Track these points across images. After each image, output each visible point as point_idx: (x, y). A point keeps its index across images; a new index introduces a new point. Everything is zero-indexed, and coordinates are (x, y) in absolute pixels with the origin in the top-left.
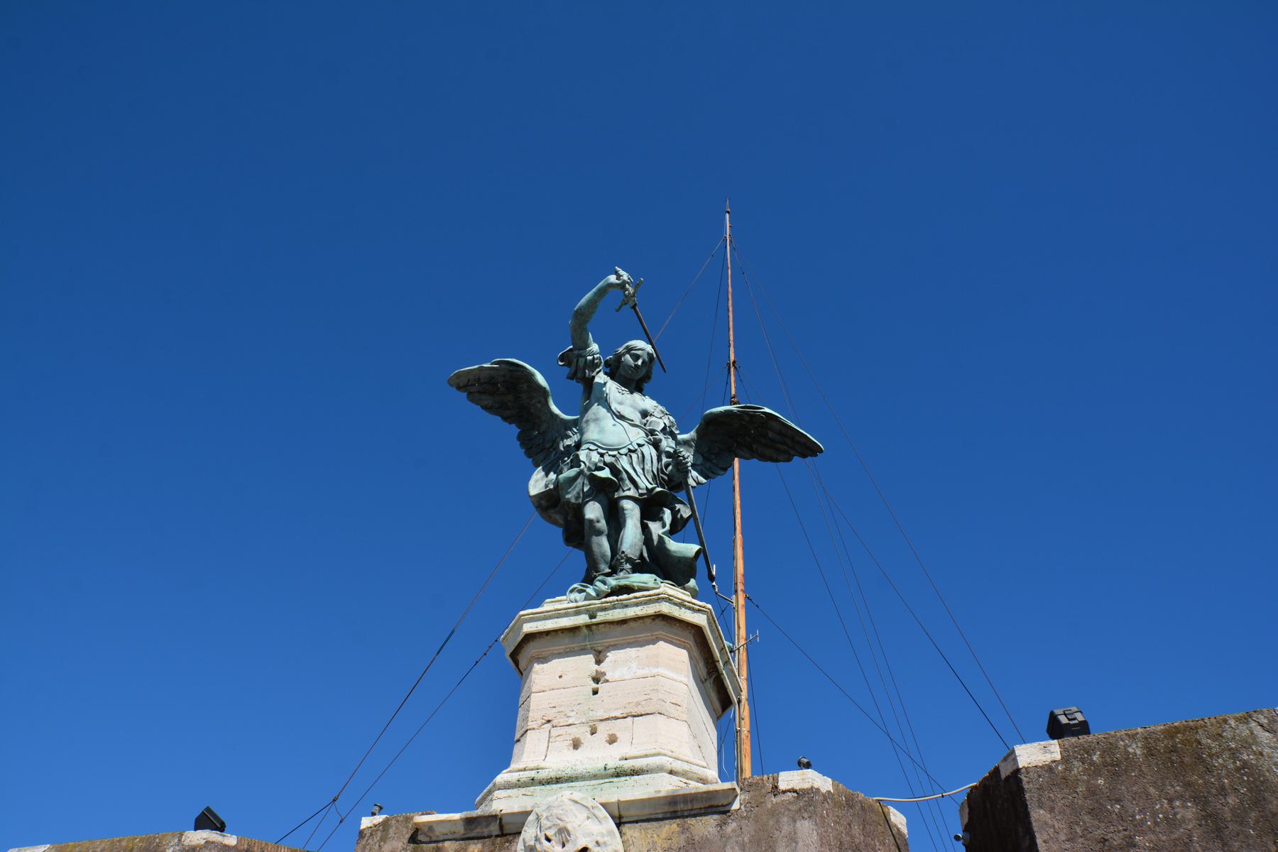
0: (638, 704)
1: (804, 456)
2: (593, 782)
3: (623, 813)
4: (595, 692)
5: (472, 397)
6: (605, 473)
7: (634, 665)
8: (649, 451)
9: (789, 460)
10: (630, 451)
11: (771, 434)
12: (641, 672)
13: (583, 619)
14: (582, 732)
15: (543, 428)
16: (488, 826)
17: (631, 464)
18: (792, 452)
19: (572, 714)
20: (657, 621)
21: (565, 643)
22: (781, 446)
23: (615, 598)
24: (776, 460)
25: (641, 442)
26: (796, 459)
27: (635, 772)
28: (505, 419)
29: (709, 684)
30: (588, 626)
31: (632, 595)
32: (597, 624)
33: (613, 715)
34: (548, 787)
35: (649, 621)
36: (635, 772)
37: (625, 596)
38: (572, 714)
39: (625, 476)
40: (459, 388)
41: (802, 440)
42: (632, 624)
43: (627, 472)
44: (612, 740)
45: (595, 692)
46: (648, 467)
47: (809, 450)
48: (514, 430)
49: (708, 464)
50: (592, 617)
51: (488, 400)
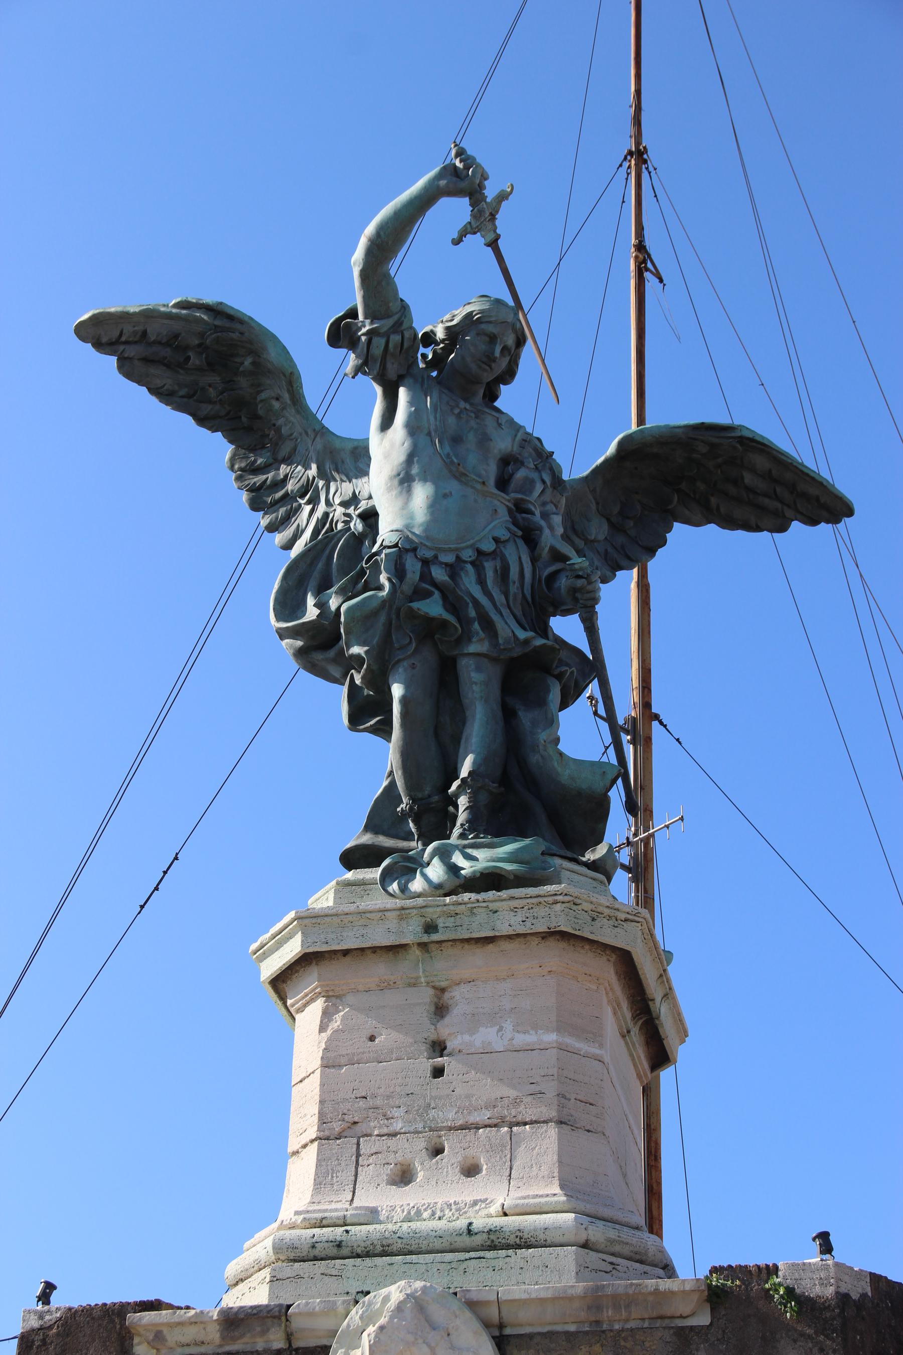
1: (813, 522)
2: (449, 1256)
3: (507, 1316)
4: (438, 1072)
5: (127, 369)
6: (433, 607)
7: (508, 1026)
8: (517, 556)
9: (782, 528)
10: (480, 552)
11: (748, 478)
12: (521, 1039)
13: (411, 933)
14: (412, 1149)
16: (264, 1332)
17: (481, 582)
18: (789, 513)
19: (396, 1113)
20: (551, 942)
21: (380, 969)
22: (767, 501)
23: (473, 896)
24: (758, 529)
25: (503, 534)
26: (796, 526)
27: (523, 1242)
28: (202, 421)
29: (636, 1036)
30: (423, 946)
31: (504, 894)
32: (440, 942)
34: (368, 1262)
35: (536, 941)
38: (396, 1113)
39: (472, 613)
40: (99, 345)
41: (813, 491)
42: (505, 945)
43: (476, 603)
44: (471, 1171)
45: (438, 1072)
46: (513, 589)
47: (824, 505)
49: (620, 539)
50: (430, 928)
51: (166, 379)
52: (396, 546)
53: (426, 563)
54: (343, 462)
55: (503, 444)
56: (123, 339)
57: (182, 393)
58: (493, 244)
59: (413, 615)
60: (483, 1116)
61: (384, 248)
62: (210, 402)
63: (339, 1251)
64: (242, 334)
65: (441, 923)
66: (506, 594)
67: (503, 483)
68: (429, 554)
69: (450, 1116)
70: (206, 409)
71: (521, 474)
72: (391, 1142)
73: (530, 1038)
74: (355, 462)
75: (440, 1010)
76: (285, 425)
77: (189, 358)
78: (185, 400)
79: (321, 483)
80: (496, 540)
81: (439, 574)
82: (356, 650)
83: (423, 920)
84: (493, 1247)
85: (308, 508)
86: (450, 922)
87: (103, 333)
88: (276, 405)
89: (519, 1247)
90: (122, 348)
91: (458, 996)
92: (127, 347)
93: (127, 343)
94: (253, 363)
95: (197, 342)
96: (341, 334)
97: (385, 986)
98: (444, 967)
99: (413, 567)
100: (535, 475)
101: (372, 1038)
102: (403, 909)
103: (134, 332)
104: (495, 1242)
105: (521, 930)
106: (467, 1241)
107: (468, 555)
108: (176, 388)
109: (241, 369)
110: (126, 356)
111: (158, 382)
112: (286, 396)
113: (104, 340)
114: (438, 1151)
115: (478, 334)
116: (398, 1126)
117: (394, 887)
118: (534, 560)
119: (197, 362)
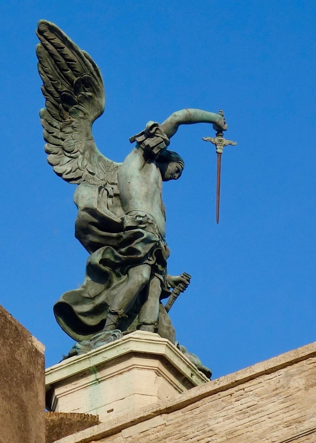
15: (68, 129)
54: (93, 157)
56: (53, 41)
57: (49, 76)
61: (189, 121)
62: (56, 89)
64: (99, 85)
70: (52, 89)
74: (98, 161)
76: (77, 123)
77: (69, 70)
78: (48, 79)
79: (80, 156)
82: (139, 248)
83: (192, 372)
86: (197, 379)
87: (47, 32)
88: (81, 115)
90: (47, 43)
92: (49, 44)
93: (52, 44)
94: (90, 96)
95: (78, 70)
101: (167, 397)
102: (190, 364)
103: (59, 43)
108: (50, 73)
109: (83, 93)
110: (47, 47)
111: (46, 64)
113: (45, 34)
115: (177, 167)
119: (70, 75)
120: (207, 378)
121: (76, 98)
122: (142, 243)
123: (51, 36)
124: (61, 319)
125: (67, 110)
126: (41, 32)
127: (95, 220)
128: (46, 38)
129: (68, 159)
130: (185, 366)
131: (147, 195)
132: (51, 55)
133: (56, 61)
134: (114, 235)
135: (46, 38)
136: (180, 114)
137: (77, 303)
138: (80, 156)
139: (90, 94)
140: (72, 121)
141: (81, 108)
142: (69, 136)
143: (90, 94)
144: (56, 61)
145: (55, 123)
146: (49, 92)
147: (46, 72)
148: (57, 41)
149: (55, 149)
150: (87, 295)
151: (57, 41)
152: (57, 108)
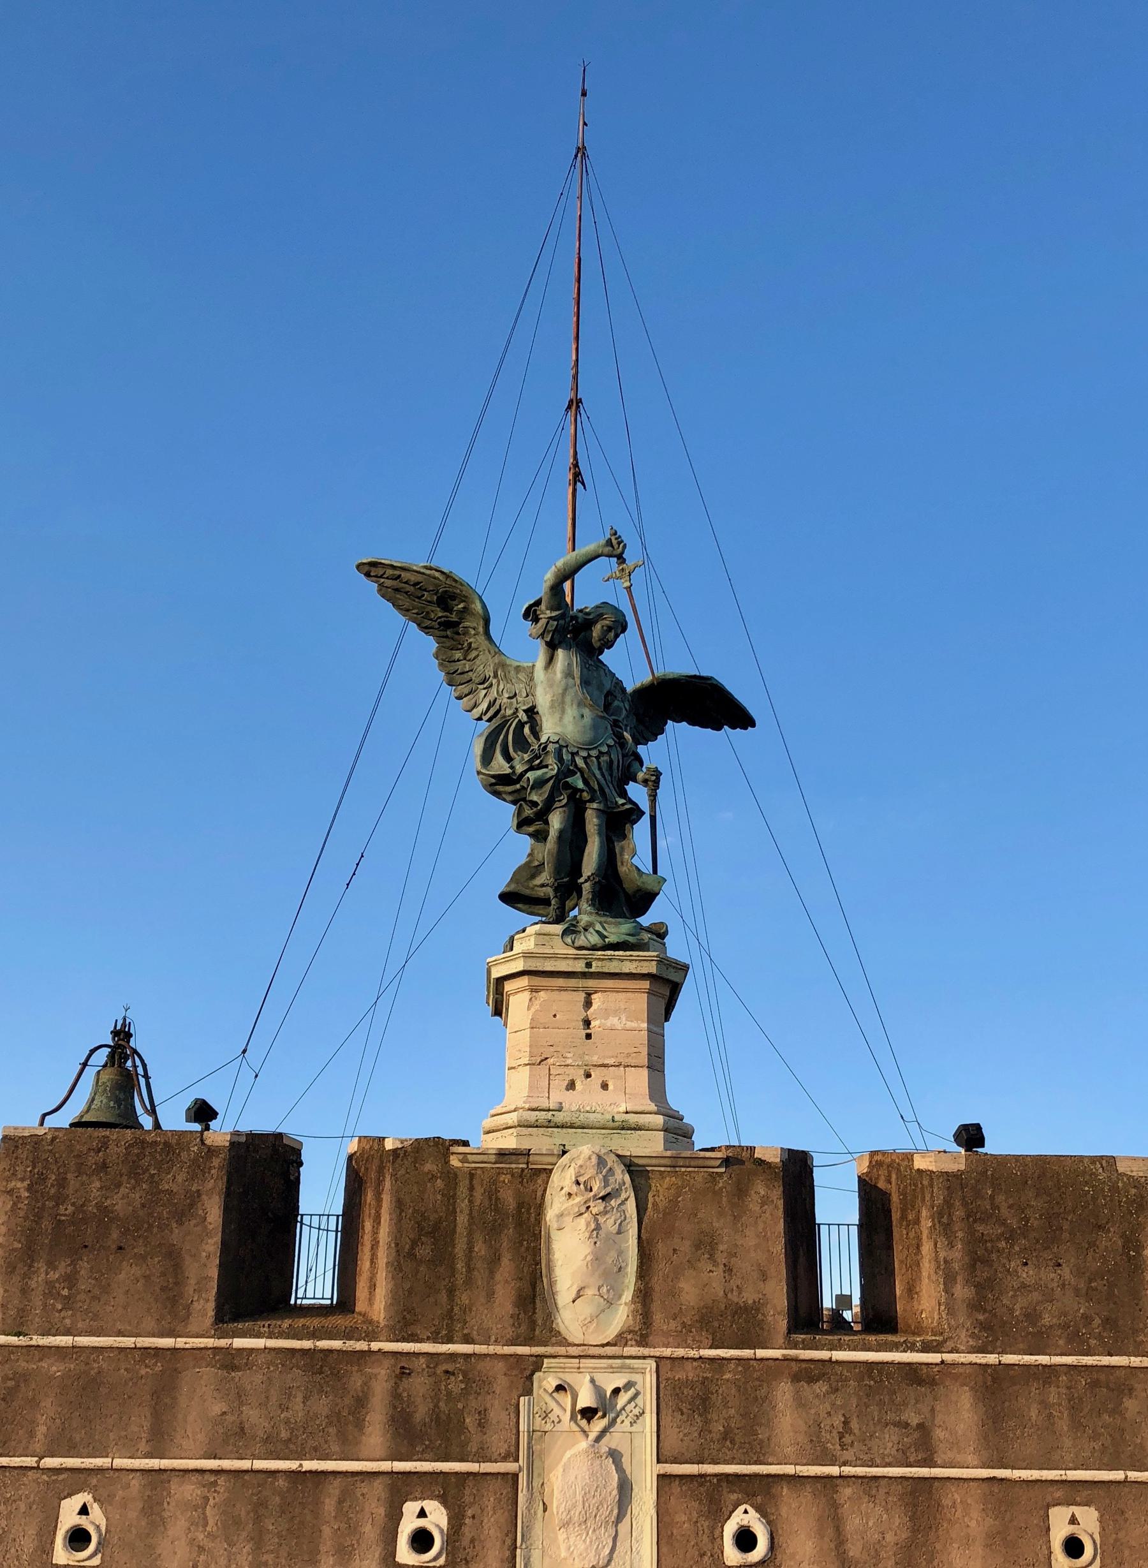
0: (628, 1055)
4: (589, 1036)
5: (383, 591)
12: (630, 1025)
13: (580, 966)
19: (569, 1055)
23: (612, 952)
27: (637, 1128)
31: (628, 953)
33: (606, 1062)
36: (637, 1128)
37: (621, 953)
38: (569, 1055)
45: (589, 1036)
48: (431, 644)
49: (641, 727)
50: (589, 965)
52: (557, 742)
53: (573, 754)
55: (608, 685)
58: (629, 589)
59: (567, 786)
60: (611, 1061)
63: (549, 1125)
65: (594, 964)
66: (611, 775)
67: (607, 707)
68: (575, 750)
69: (595, 1059)
70: (428, 623)
71: (616, 703)
72: (565, 1069)
73: (634, 1025)
75: (588, 1004)
79: (494, 681)
80: (609, 746)
81: (580, 763)
82: (535, 798)
84: (623, 1129)
85: (484, 692)
88: (473, 632)
89: (635, 1129)
91: (596, 998)
96: (531, 614)
97: (562, 989)
98: (591, 983)
99: (566, 757)
100: (621, 704)
101: (555, 1016)
104: (624, 1127)
105: (634, 971)
106: (611, 1124)
107: (594, 753)
112: (481, 630)
114: (588, 1076)
116: (569, 1061)
117: (569, 940)
118: (623, 756)
120: (617, 953)
121: (454, 618)
122: (534, 792)
123: (380, 571)
124: (520, 905)
125: (458, 634)
126: (368, 575)
127: (493, 781)
128: (376, 576)
129: (484, 692)
130: (571, 962)
131: (552, 707)
132: (397, 590)
133: (406, 593)
134: (518, 786)
135: (376, 576)
136: (549, 576)
137: (533, 877)
138: (494, 681)
139: (461, 606)
140: (470, 644)
141: (467, 624)
142: (477, 661)
143: (461, 606)
144: (406, 593)
145: (458, 655)
146: (426, 628)
147: (408, 610)
148: (390, 572)
149: (464, 689)
150: (536, 863)
151: (390, 572)
152: (447, 637)
